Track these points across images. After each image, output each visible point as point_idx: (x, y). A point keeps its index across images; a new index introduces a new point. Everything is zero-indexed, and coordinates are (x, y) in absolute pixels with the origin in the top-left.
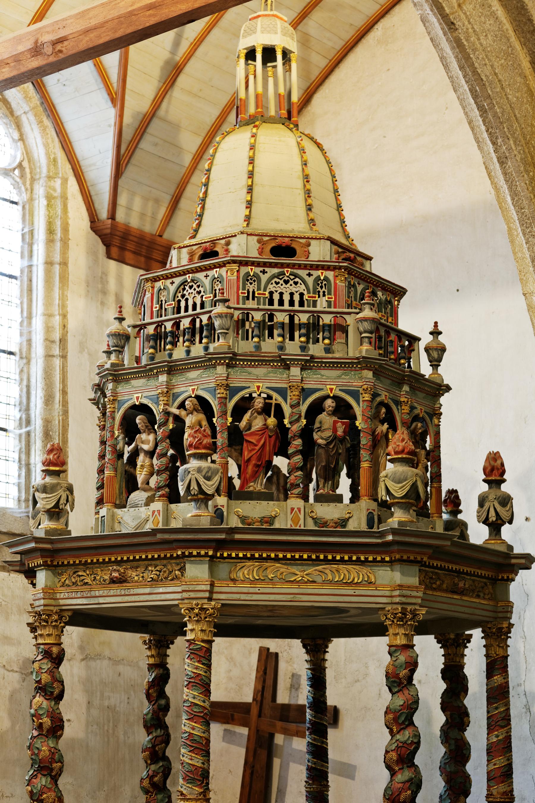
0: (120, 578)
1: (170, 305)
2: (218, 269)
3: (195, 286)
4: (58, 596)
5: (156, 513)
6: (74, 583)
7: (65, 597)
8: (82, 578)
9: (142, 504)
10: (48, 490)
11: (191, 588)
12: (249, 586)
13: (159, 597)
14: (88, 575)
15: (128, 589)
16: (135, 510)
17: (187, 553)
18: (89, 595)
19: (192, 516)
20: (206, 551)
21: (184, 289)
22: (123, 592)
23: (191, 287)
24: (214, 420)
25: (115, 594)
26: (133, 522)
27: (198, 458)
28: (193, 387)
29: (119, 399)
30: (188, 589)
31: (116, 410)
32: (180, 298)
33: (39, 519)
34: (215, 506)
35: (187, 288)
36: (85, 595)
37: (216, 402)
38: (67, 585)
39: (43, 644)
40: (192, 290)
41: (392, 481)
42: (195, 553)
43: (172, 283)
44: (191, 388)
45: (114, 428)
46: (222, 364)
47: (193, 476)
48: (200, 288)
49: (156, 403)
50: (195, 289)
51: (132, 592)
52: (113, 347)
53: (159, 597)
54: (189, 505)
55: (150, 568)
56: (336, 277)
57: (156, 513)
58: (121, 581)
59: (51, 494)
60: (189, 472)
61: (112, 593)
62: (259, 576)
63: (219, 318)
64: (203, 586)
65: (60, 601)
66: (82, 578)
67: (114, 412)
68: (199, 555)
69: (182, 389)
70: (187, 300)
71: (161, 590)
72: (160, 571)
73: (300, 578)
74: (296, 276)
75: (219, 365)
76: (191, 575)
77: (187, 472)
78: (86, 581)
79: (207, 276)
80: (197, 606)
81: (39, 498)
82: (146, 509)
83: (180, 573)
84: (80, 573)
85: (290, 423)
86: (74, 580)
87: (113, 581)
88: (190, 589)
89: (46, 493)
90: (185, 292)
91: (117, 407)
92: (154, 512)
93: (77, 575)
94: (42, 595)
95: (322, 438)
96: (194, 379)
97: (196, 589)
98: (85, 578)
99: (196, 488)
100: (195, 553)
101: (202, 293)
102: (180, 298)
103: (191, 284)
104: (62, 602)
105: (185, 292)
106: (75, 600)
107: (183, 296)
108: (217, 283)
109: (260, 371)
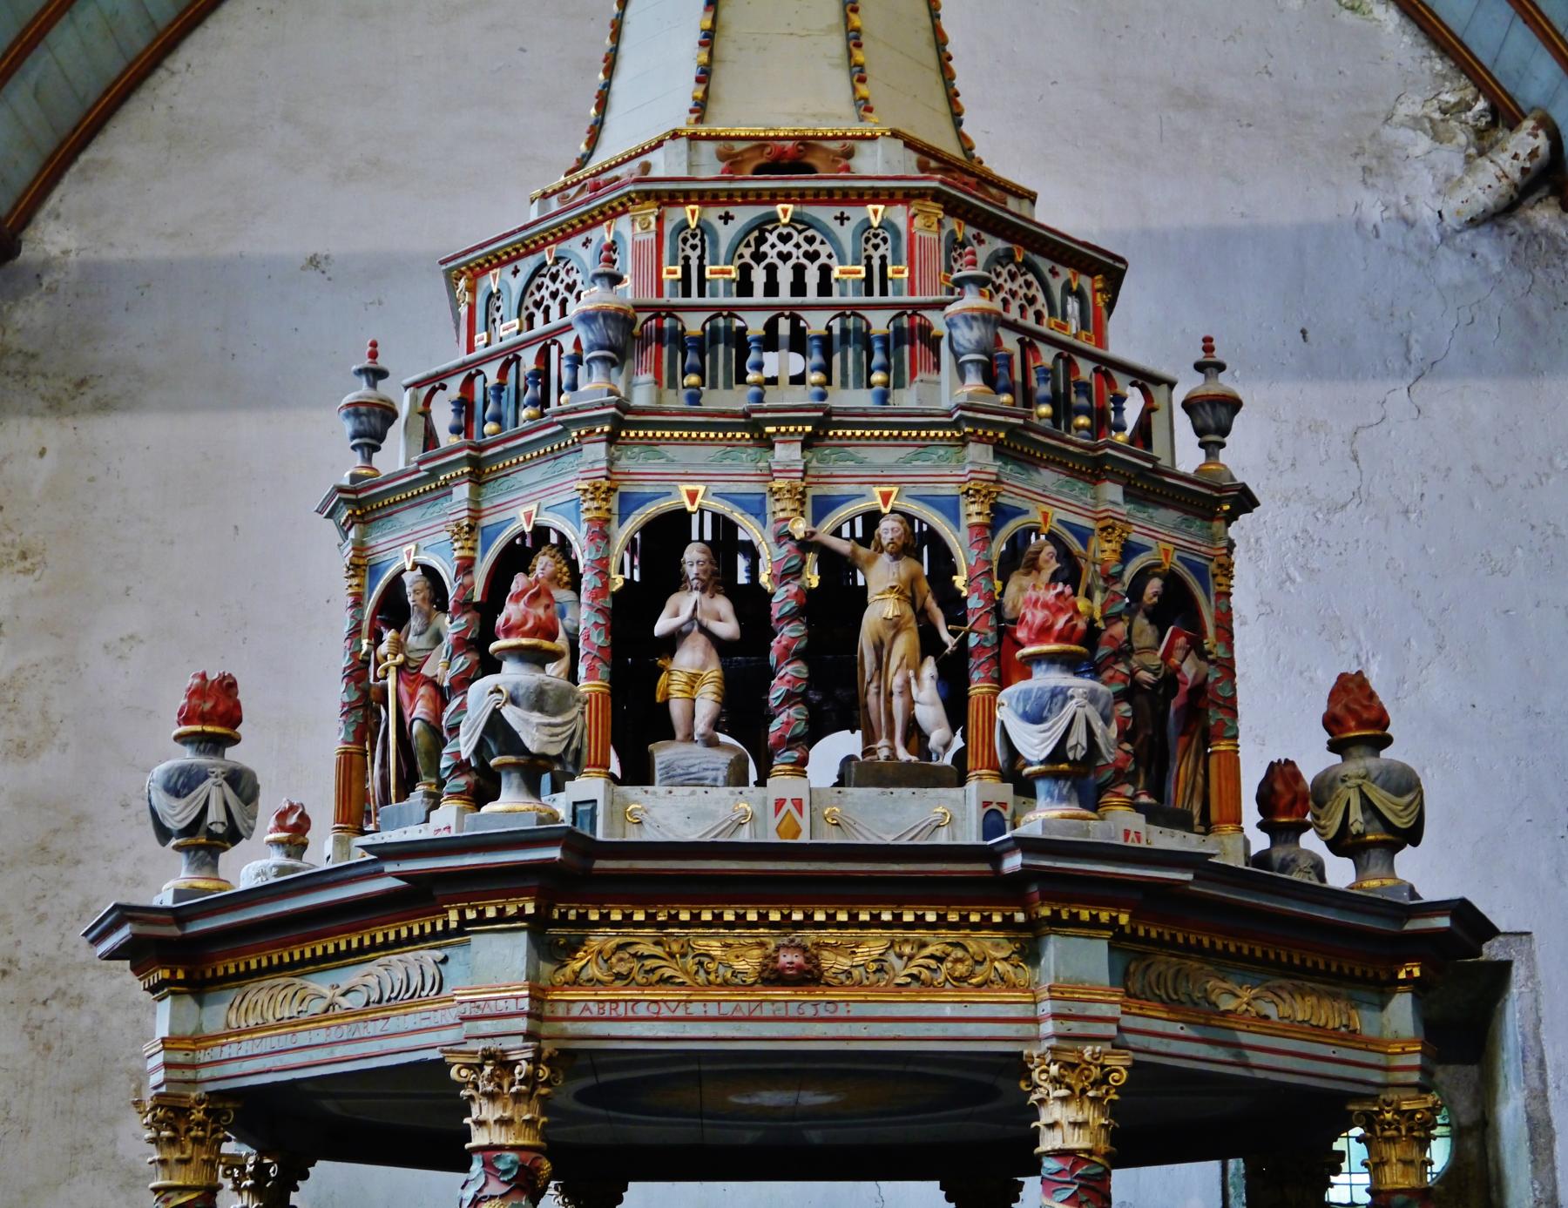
0: (809, 972)
1: (721, 272)
2: (881, 208)
3: (797, 238)
4: (561, 1011)
5: (788, 805)
6: (619, 976)
7: (587, 1014)
8: (650, 963)
9: (715, 780)
10: (550, 703)
11: (1076, 1008)
12: (1165, 1015)
13: (937, 1030)
14: (672, 955)
15: (829, 1002)
16: (693, 793)
17: (1065, 916)
18: (680, 1013)
19: (1063, 817)
20: (1114, 914)
21: (761, 240)
22: (809, 1011)
23: (785, 239)
24: (959, 581)
25: (782, 1013)
26: (686, 824)
27: (1062, 664)
28: (885, 489)
29: (622, 489)
30: (1066, 1012)
31: (615, 519)
32: (747, 259)
33: (203, 796)
34: (986, 804)
35: (772, 238)
36: (665, 1012)
37: (965, 533)
38: (590, 980)
39: (513, 1148)
40: (787, 248)
41: (1383, 787)
42: (1085, 915)
43: (727, 218)
44: (877, 490)
45: (607, 565)
46: (989, 441)
47: (1080, 711)
48: (816, 246)
49: (757, 516)
50: (798, 246)
51: (842, 1011)
52: (591, 349)
53: (937, 1030)
54: (883, 793)
55: (907, 950)
56: (1095, 291)
57: (788, 805)
58: (809, 977)
59: (554, 715)
60: (1067, 699)
61: (767, 1010)
62: (1176, 993)
63: (981, 324)
64: (1104, 1006)
65: (565, 1024)
66: (650, 963)
67: (608, 521)
68: (1094, 923)
69: (846, 489)
70: (771, 270)
71: (948, 1011)
72: (940, 960)
73: (1245, 1006)
74: (1031, 267)
75: (980, 440)
76: (1068, 975)
77: (1060, 697)
78: (668, 972)
79: (842, 219)
80: (1097, 1059)
81: (527, 722)
82: (732, 793)
83: (1009, 968)
84: (646, 948)
85: (1105, 618)
86: (623, 968)
87: (773, 977)
88: (1074, 1012)
89: (542, 710)
90: (765, 248)
91: (615, 510)
92: (780, 803)
93: (634, 955)
94: (525, 1004)
95: (1146, 669)
96: (889, 467)
97: (1088, 1013)
98: (663, 963)
99: (1084, 743)
100: (1085, 915)
101: (823, 260)
102: (747, 259)
103: (785, 231)
104: (572, 1028)
105: (765, 248)
106: (627, 1024)
107: (759, 257)
108: (874, 241)
109: (1047, 478)
